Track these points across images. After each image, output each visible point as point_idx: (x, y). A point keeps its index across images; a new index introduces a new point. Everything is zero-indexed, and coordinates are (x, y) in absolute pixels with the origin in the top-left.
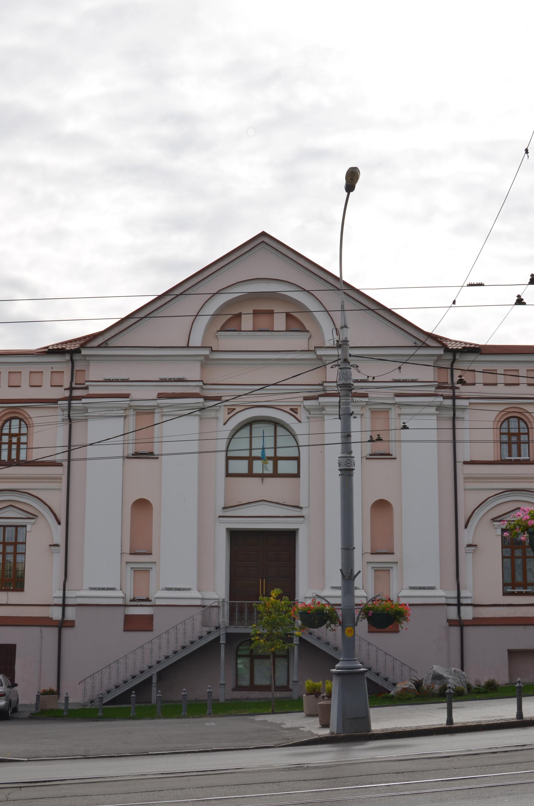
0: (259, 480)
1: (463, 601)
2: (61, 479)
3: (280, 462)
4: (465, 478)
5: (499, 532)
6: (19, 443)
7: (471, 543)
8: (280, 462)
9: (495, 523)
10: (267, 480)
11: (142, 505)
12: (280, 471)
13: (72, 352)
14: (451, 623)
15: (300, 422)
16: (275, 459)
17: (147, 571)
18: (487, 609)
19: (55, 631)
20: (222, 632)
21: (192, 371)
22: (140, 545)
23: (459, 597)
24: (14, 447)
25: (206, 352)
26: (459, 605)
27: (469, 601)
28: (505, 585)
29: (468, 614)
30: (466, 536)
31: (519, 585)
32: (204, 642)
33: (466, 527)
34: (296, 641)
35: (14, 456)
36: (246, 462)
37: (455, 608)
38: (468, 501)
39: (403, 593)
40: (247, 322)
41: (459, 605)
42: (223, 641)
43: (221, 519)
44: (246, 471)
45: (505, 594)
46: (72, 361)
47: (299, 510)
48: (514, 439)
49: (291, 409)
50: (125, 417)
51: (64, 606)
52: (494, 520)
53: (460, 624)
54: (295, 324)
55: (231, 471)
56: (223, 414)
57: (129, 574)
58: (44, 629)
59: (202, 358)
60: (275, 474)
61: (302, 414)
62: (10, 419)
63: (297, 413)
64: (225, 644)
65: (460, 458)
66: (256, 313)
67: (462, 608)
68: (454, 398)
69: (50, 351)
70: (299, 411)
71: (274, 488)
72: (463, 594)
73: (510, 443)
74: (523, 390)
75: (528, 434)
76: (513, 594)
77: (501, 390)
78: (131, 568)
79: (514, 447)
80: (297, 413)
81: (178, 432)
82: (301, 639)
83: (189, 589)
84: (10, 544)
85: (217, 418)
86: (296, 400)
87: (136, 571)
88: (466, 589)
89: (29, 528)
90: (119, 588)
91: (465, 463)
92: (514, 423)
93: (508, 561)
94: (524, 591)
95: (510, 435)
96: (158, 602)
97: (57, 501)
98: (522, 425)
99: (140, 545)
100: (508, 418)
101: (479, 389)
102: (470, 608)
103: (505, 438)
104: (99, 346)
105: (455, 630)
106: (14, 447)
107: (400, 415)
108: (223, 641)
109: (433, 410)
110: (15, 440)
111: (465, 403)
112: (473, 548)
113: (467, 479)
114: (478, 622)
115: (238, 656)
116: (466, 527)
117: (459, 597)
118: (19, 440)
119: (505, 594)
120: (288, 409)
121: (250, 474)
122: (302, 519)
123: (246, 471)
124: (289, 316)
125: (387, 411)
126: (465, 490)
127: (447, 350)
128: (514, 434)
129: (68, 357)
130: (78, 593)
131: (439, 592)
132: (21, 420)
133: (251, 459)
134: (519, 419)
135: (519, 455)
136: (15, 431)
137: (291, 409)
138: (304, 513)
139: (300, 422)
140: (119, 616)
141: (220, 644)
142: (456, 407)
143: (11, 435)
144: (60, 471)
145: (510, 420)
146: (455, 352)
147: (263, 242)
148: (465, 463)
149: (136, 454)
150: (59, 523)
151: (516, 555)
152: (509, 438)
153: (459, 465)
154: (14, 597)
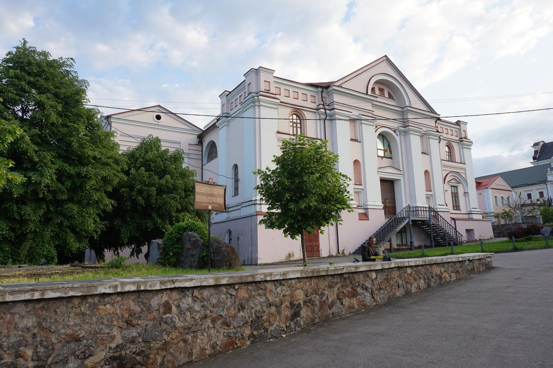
6: (297, 127)
21: (369, 106)
24: (295, 128)
28: (454, 206)
39: (438, 207)
45: (454, 209)
46: (322, 92)
52: (449, 181)
53: (454, 219)
54: (390, 97)
60: (385, 157)
62: (292, 115)
104: (338, 86)
105: (453, 221)
118: (297, 125)
119: (454, 209)
124: (389, 94)
129: (320, 89)
143: (293, 123)
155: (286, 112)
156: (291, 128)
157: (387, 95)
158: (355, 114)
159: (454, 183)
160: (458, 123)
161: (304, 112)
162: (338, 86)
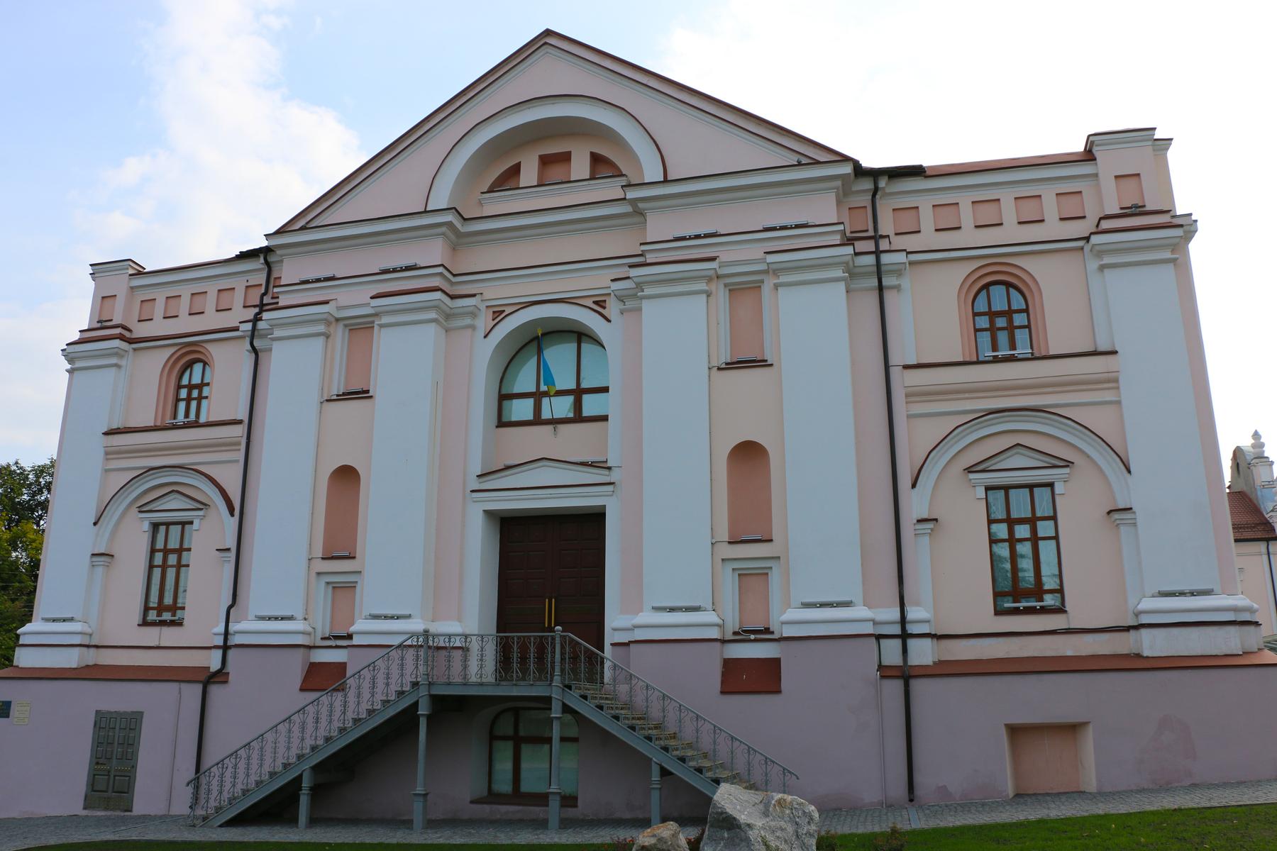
0: (550, 427)
1: (912, 629)
2: (239, 444)
3: (586, 398)
4: (907, 396)
5: (981, 492)
6: (200, 398)
7: (925, 516)
8: (586, 398)
9: (972, 476)
10: (561, 427)
11: (346, 476)
12: (587, 412)
13: (266, 251)
14: (886, 672)
15: (609, 321)
16: (578, 393)
17: (352, 587)
18: (964, 642)
19: (198, 688)
20: (423, 692)
22: (339, 545)
23: (903, 620)
24: (194, 404)
25: (449, 217)
26: (905, 636)
27: (925, 629)
28: (997, 595)
29: (922, 653)
30: (915, 504)
31: (1027, 594)
32: (391, 712)
33: (914, 486)
34: (556, 712)
35: (192, 417)
36: (531, 401)
37: (897, 643)
38: (916, 438)
40: (529, 175)
41: (905, 636)
42: (423, 710)
43: (475, 495)
44: (530, 416)
45: (999, 612)
47: (606, 472)
48: (1001, 322)
49: (595, 303)
50: (328, 336)
51: (225, 648)
52: (970, 470)
53: (906, 675)
55: (505, 419)
56: (484, 321)
57: (322, 594)
58: (184, 686)
59: (444, 229)
61: (613, 308)
63: (604, 308)
64: (429, 717)
65: (895, 359)
66: (546, 161)
67: (912, 643)
68: (877, 253)
69: (244, 256)
70: (607, 304)
71: (574, 441)
72: (912, 614)
73: (993, 330)
74: (1011, 232)
75: (1026, 311)
76: (1016, 611)
77: (968, 237)
78: (328, 583)
79: (1003, 337)
80: (604, 308)
81: (409, 357)
82: (566, 709)
83: (409, 616)
84: (173, 551)
85: (473, 327)
86: (598, 281)
87: (336, 587)
88: (918, 604)
89: (196, 522)
90: (299, 614)
91: (906, 367)
92: (998, 293)
93: (1003, 551)
94: (1038, 605)
95: (992, 315)
96: (356, 641)
97: (230, 478)
98: (1018, 302)
99: (339, 545)
100: (986, 287)
101: (928, 238)
102: (928, 641)
103: (983, 322)
105: (896, 686)
106: (194, 404)
107: (776, 286)
108: (423, 710)
109: (839, 273)
110: (195, 393)
111: (901, 258)
112: (931, 525)
113: (910, 395)
114: (944, 670)
115: (493, 738)
116: (914, 486)
117: (903, 620)
119: (999, 612)
120: (589, 303)
121: (537, 421)
122: (610, 488)
123: (530, 416)
124: (596, 159)
125: (757, 287)
126: (909, 417)
127: (859, 171)
128: (1000, 314)
130: (246, 627)
131: (860, 612)
132: (205, 364)
133: (538, 396)
134: (1008, 285)
135: (1013, 347)
136: (196, 380)
137: (596, 303)
138: (614, 476)
139: (609, 321)
140: (295, 668)
141: (418, 717)
142: (883, 268)
143: (191, 387)
144: (239, 431)
145: (991, 288)
146: (875, 174)
147: (546, 43)
148: (906, 367)
149: (344, 394)
150: (232, 515)
151: (1018, 536)
152: (992, 322)
153: (895, 373)
154: (169, 636)
155: (154, 363)
156: (182, 405)
157: (580, 167)
158: (354, 300)
159: (1019, 468)
160: (1088, 155)
161: (208, 346)
162: (303, 228)
